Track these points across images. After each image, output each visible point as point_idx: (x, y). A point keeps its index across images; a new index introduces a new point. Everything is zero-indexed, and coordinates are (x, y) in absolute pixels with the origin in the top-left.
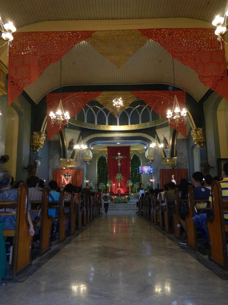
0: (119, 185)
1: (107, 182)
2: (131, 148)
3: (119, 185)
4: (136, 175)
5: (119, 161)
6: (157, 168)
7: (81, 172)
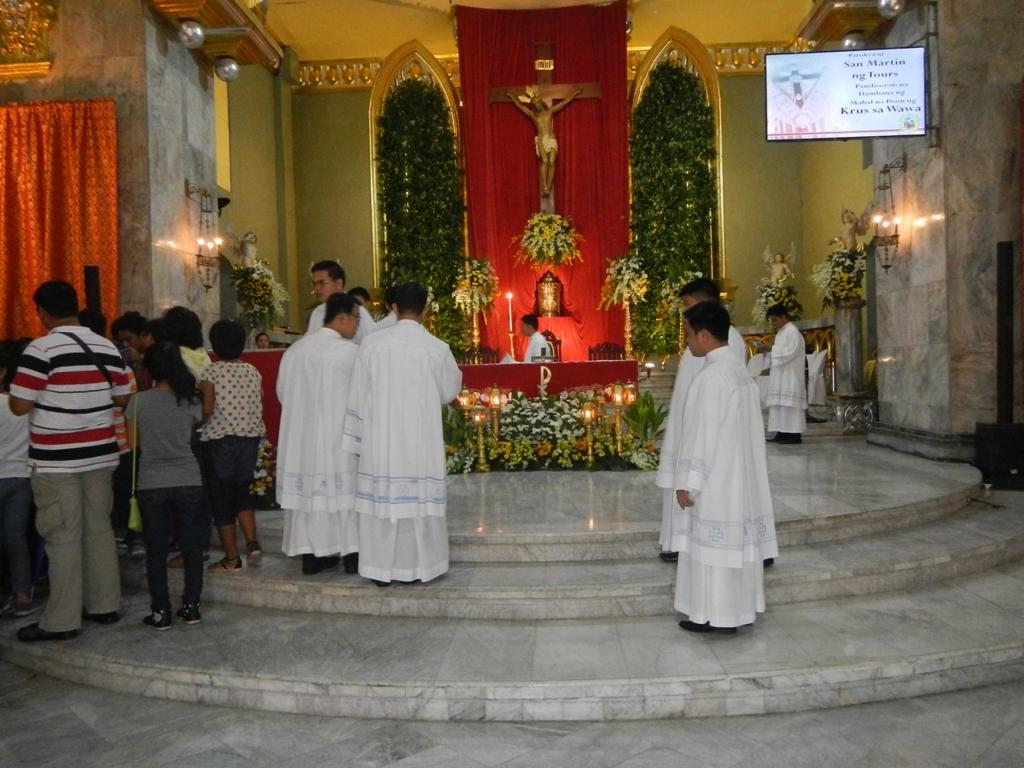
0: (549, 302)
1: (453, 280)
2: (629, 14)
3: (549, 302)
4: (673, 218)
5: (544, 121)
6: (982, 70)
7: (107, 133)
